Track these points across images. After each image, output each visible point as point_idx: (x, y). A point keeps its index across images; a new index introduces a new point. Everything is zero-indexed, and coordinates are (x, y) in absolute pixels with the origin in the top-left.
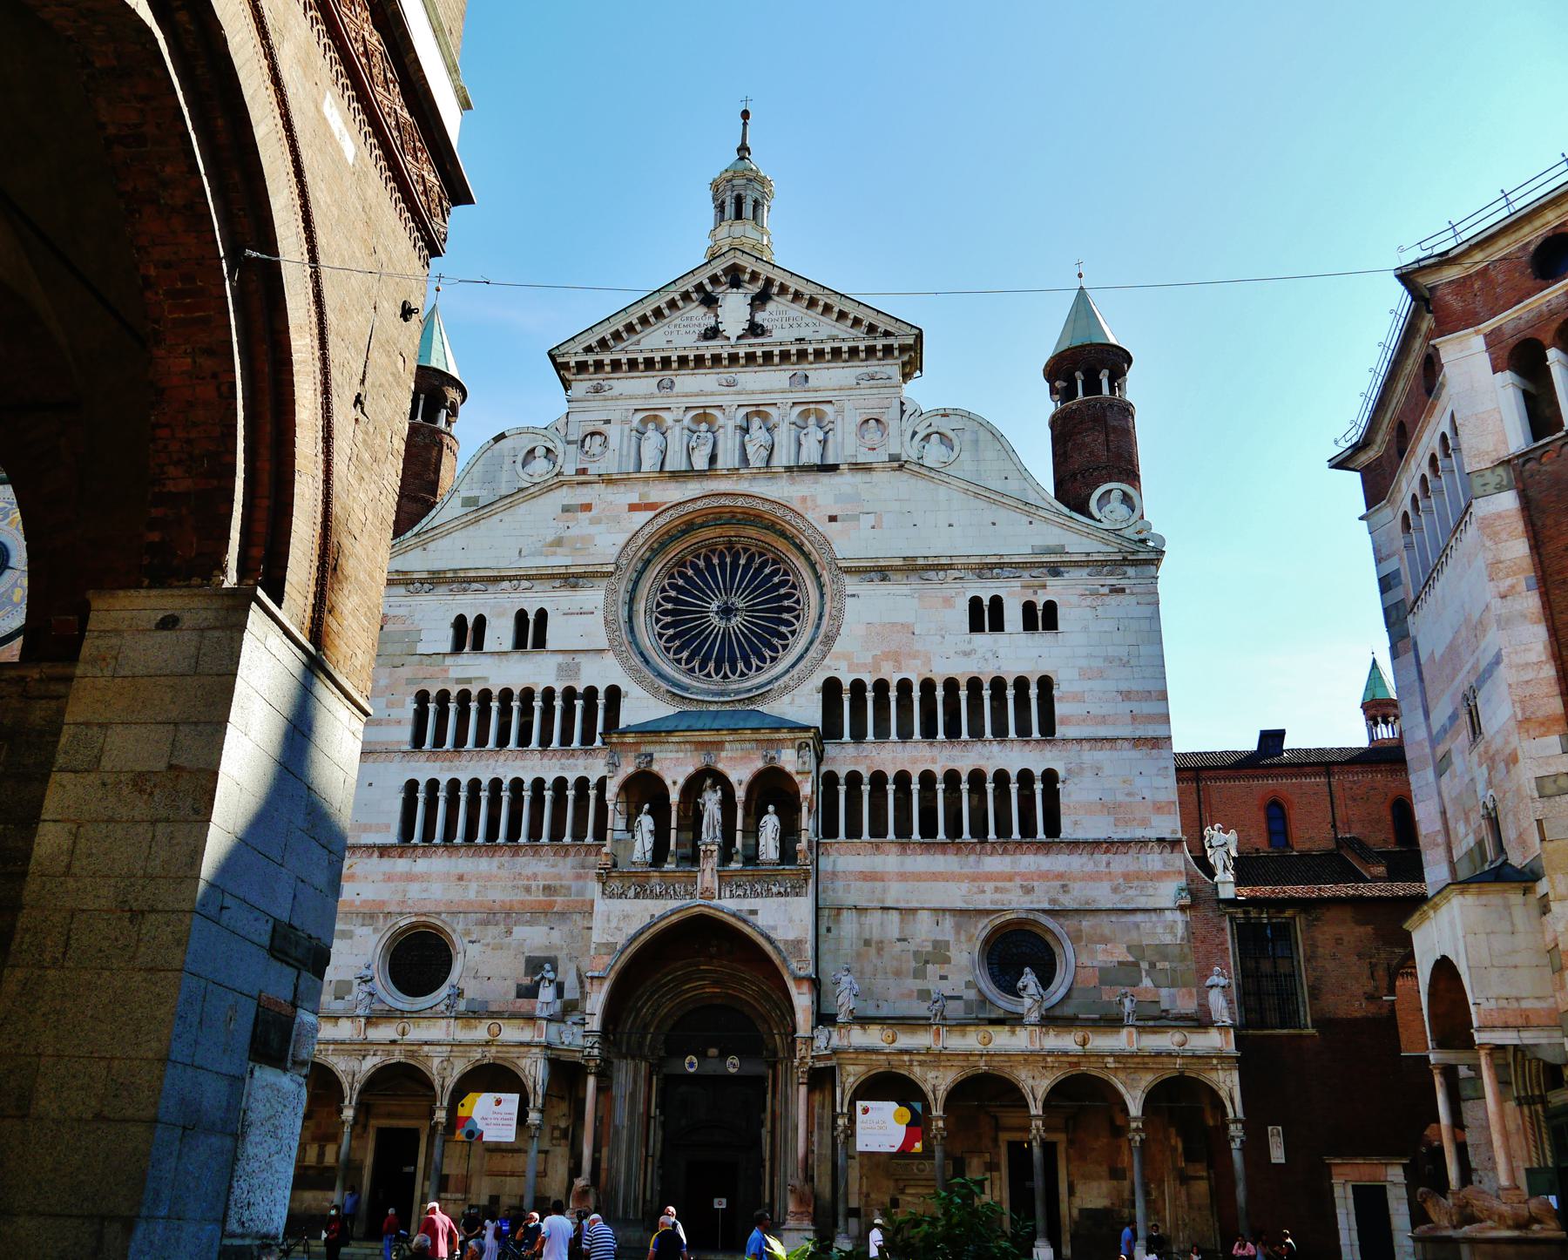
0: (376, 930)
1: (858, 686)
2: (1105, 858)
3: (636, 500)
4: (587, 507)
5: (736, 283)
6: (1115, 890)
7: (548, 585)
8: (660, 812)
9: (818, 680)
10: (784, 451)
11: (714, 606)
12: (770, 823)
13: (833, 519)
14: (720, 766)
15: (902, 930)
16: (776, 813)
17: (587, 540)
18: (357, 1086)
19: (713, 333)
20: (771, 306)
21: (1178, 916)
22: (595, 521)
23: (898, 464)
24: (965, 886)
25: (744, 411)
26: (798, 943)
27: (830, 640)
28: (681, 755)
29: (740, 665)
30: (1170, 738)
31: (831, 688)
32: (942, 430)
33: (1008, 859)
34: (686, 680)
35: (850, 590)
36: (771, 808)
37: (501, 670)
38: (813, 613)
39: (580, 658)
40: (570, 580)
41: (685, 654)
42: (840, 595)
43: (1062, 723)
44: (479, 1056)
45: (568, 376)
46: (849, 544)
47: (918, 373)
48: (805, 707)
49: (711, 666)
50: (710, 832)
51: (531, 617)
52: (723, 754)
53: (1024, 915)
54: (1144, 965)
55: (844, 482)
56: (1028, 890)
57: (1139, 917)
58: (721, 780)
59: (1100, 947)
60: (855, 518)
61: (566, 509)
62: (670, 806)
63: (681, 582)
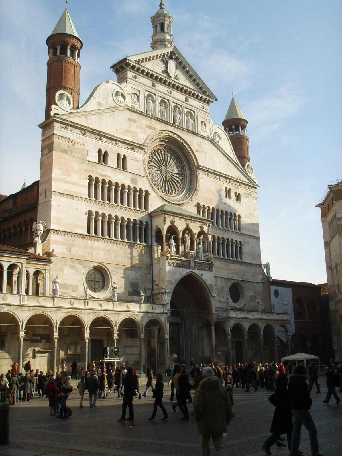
0: (84, 267)
2: (250, 267)
3: (148, 125)
4: (135, 121)
5: (171, 58)
6: (252, 276)
7: (126, 146)
8: (176, 240)
17: (136, 133)
18: (118, 326)
21: (261, 284)
22: (137, 127)
24: (226, 271)
26: (212, 285)
28: (181, 222)
30: (260, 238)
31: (198, 206)
33: (234, 265)
35: (202, 176)
37: (111, 174)
39: (137, 177)
40: (133, 146)
43: (242, 229)
44: (151, 316)
45: (125, 67)
48: (192, 210)
51: (122, 157)
53: (236, 281)
54: (256, 296)
56: (238, 274)
57: (256, 284)
59: (249, 291)
61: (129, 119)
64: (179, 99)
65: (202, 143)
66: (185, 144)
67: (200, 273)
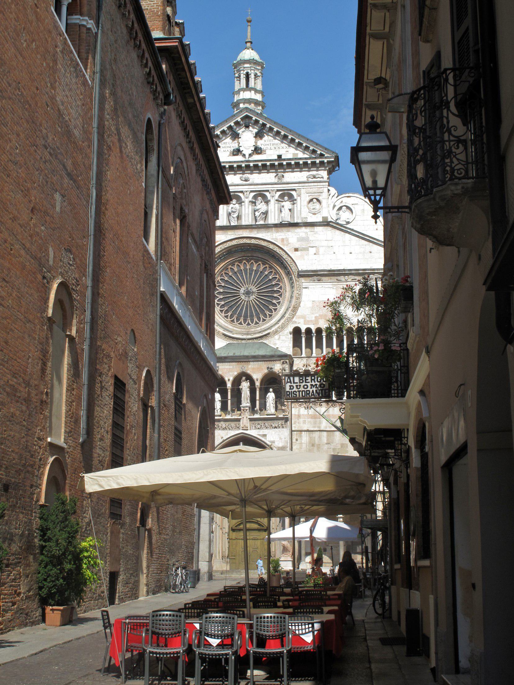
1: (309, 331)
8: (224, 393)
9: (290, 328)
10: (273, 214)
11: (242, 290)
12: (271, 396)
13: (296, 250)
14: (249, 372)
15: (328, 440)
16: (274, 392)
19: (237, 152)
20: (266, 138)
23: (326, 223)
25: (252, 194)
27: (295, 309)
28: (231, 367)
29: (255, 319)
31: (297, 332)
32: (346, 205)
34: (230, 327)
36: (271, 390)
38: (288, 294)
41: (229, 314)
42: (300, 288)
46: (304, 263)
47: (337, 168)
49: (242, 320)
50: (246, 403)
52: (250, 366)
55: (302, 231)
58: (249, 378)
60: (306, 249)
62: (227, 390)
63: (226, 279)
64: (264, 182)
65: (309, 233)
66: (271, 246)
67: (261, 433)
